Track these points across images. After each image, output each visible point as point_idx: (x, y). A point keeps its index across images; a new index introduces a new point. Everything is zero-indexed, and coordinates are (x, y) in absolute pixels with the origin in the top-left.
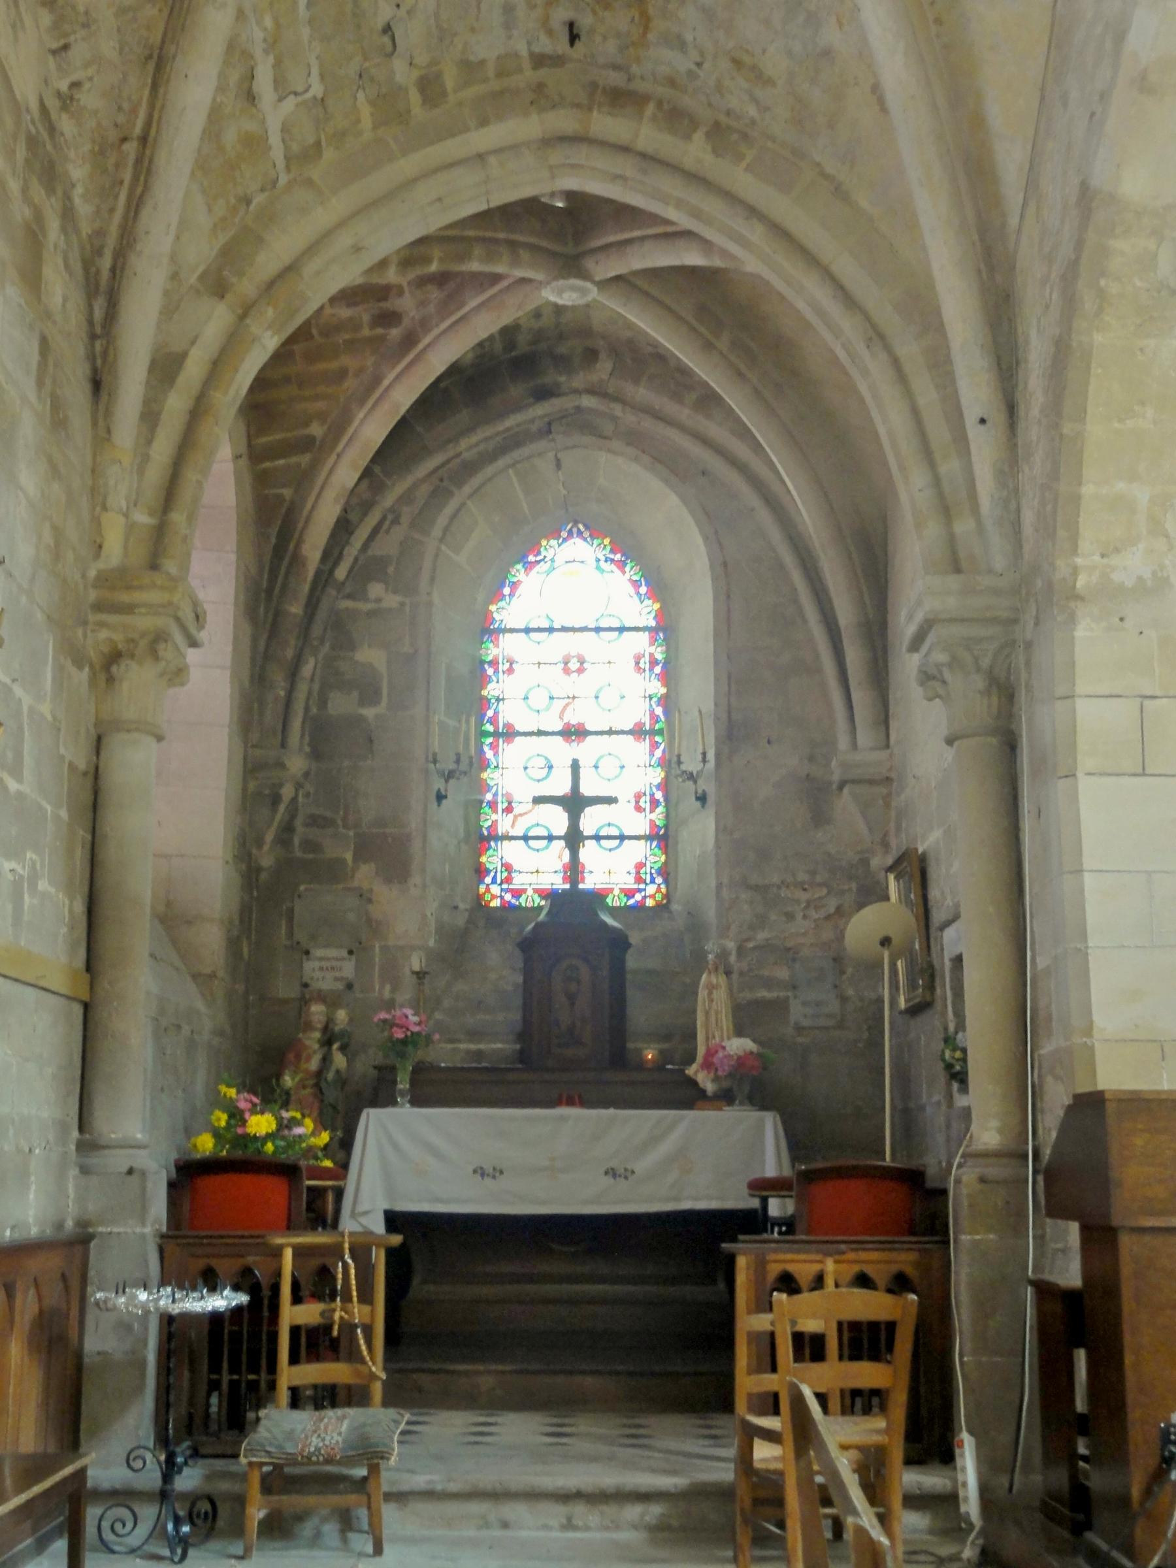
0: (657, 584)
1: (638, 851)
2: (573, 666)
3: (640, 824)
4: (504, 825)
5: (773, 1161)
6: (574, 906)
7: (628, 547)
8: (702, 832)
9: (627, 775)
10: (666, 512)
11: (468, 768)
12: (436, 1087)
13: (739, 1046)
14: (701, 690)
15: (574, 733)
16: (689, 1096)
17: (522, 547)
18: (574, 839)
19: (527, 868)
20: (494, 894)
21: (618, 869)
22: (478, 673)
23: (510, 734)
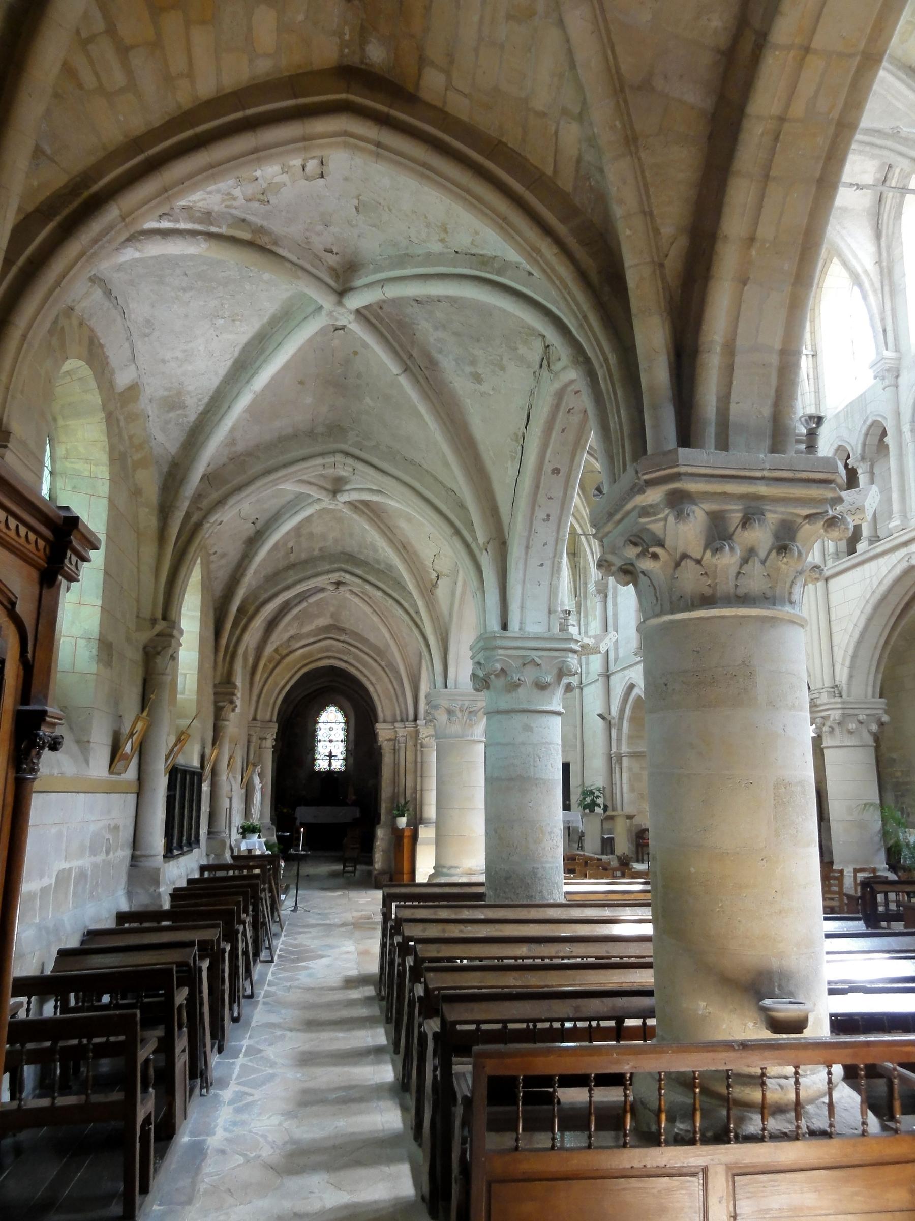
0: (346, 715)
1: (342, 761)
2: (331, 729)
3: (342, 757)
4: (318, 757)
5: (358, 815)
6: (330, 774)
7: (341, 708)
8: (351, 760)
9: (339, 750)
10: (347, 705)
11: (312, 749)
12: (308, 803)
13: (354, 797)
14: (352, 737)
15: (331, 741)
16: (346, 805)
17: (323, 708)
18: (330, 759)
19: (322, 764)
20: (317, 768)
21: (338, 765)
22: (315, 731)
23: (320, 741)
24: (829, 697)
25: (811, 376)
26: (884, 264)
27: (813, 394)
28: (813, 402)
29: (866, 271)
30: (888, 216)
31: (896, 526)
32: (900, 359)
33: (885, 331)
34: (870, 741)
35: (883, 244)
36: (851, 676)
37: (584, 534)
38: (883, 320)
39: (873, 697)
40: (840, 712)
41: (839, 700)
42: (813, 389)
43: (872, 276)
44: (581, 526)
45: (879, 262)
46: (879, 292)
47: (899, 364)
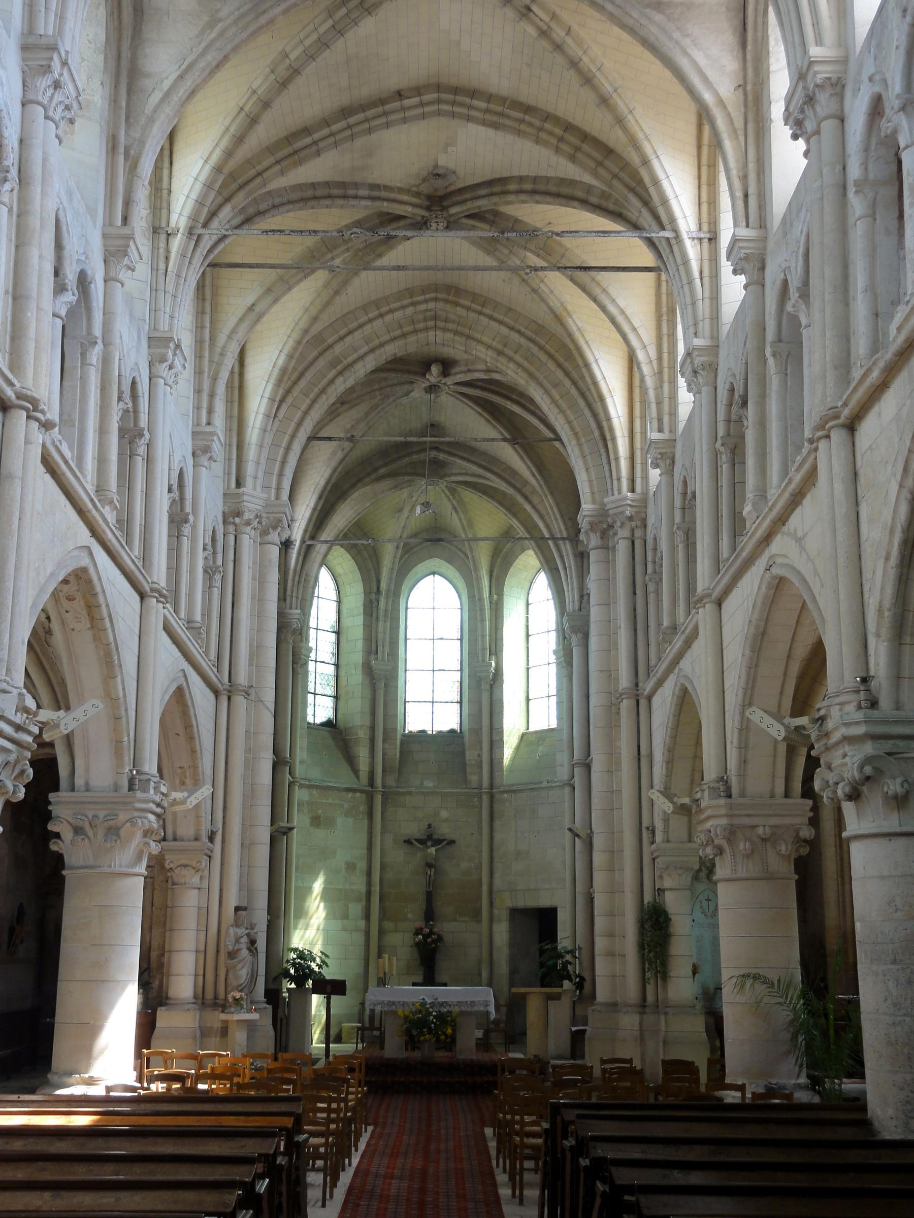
24: (710, 798)
25: (706, 273)
26: (749, 88)
27: (707, 301)
28: (707, 315)
29: (721, 102)
30: (756, 10)
31: (749, 513)
32: (765, 239)
33: (746, 196)
34: (787, 869)
35: (749, 56)
36: (743, 762)
37: (553, 538)
38: (744, 178)
39: (787, 796)
40: (724, 821)
41: (722, 801)
42: (707, 294)
43: (730, 108)
44: (547, 526)
45: (742, 86)
46: (741, 134)
47: (765, 248)
